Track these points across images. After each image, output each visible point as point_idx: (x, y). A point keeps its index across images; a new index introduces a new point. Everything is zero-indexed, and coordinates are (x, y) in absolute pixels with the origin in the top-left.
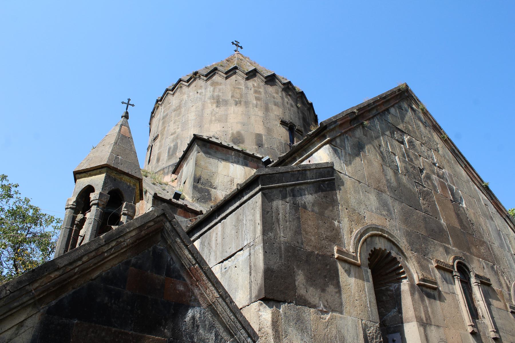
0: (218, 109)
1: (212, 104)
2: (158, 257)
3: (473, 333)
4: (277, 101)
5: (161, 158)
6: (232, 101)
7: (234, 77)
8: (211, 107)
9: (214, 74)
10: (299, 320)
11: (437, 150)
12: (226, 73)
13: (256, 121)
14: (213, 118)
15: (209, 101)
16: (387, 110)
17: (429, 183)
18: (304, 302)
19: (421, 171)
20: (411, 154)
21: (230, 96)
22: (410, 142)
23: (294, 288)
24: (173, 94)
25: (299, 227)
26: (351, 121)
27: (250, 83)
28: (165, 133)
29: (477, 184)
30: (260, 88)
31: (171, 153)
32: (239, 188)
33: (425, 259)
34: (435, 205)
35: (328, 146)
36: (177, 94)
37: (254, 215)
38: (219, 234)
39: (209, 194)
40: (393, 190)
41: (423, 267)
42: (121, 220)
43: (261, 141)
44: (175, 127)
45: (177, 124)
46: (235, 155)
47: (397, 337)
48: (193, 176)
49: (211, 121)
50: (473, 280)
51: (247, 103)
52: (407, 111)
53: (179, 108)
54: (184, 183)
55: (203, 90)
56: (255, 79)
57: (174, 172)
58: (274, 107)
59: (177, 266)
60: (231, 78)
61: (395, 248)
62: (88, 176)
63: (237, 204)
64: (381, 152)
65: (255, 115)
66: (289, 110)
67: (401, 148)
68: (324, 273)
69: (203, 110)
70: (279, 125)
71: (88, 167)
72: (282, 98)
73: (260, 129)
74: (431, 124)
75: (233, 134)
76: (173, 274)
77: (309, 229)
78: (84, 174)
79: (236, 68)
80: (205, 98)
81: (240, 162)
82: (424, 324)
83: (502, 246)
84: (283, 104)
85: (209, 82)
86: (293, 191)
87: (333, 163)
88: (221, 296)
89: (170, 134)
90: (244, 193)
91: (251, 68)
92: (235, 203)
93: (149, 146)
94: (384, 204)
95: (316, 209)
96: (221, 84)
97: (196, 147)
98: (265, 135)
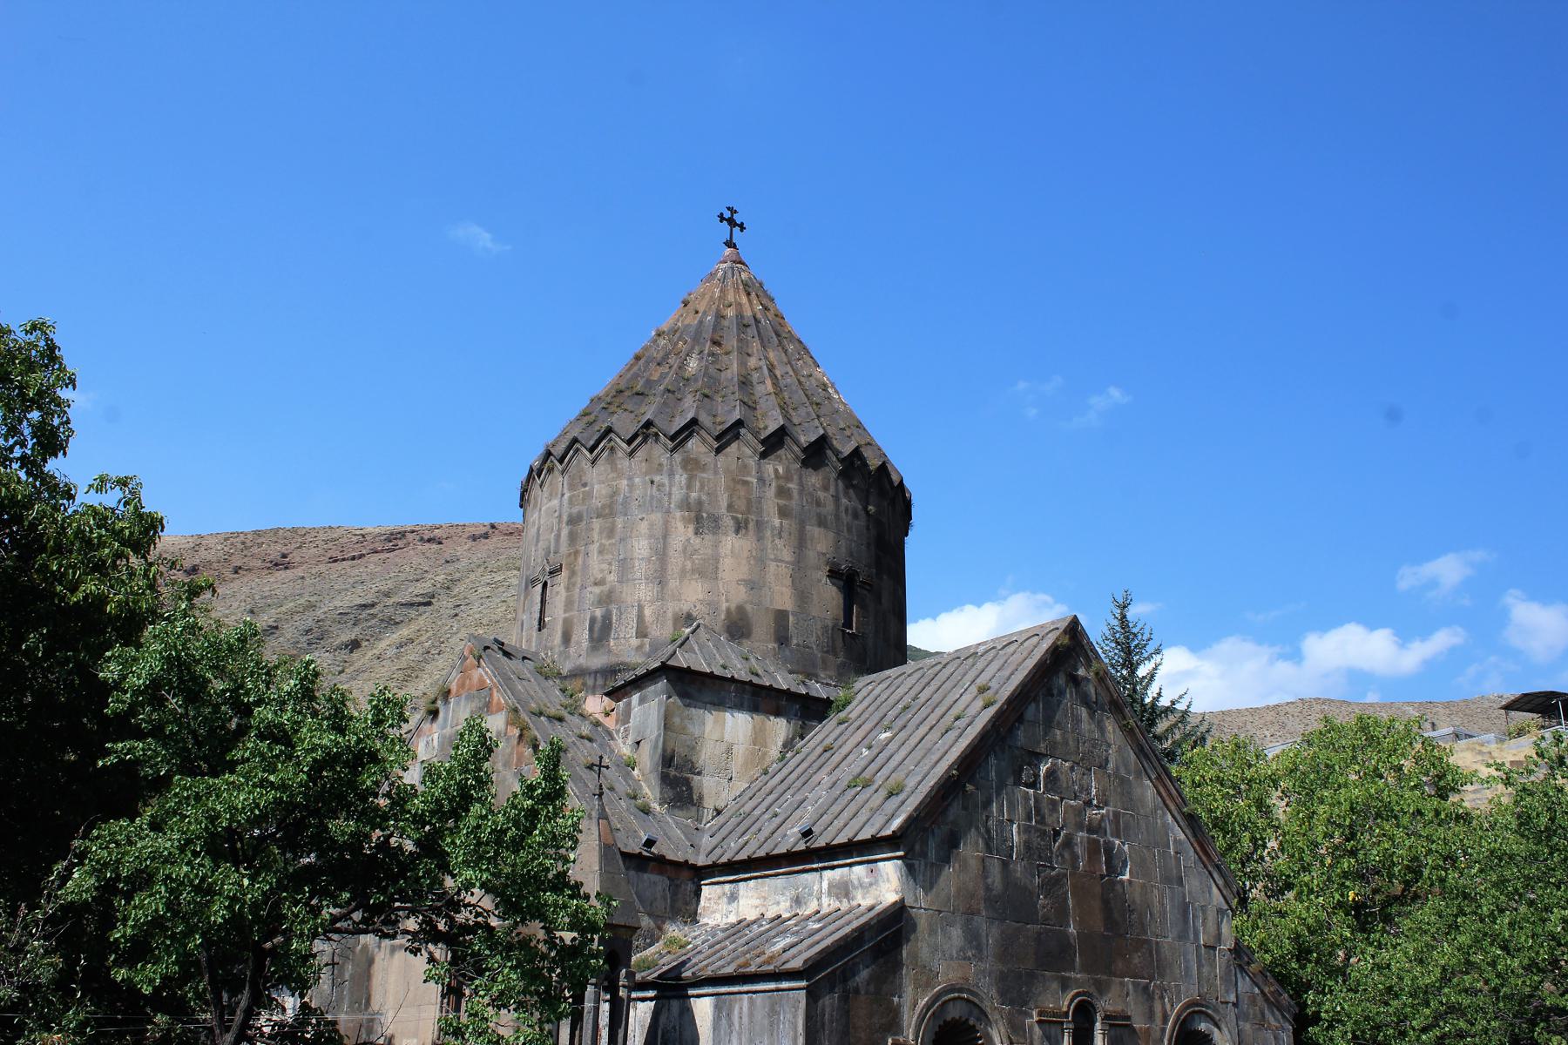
0: (698, 540)
1: (686, 521)
4: (824, 511)
5: (574, 638)
6: (728, 522)
7: (734, 445)
8: (682, 533)
11: (1103, 766)
12: (718, 438)
14: (689, 565)
15: (678, 514)
16: (1021, 719)
17: (1067, 855)
19: (1057, 834)
20: (1044, 804)
21: (724, 503)
22: (1051, 774)
24: (593, 462)
26: (944, 798)
27: (771, 467)
29: (1173, 807)
30: (788, 478)
33: (1021, 1012)
34: (1066, 899)
36: (602, 465)
37: (795, 1017)
38: (745, 1009)
39: (690, 789)
40: (991, 900)
48: (660, 751)
50: (1098, 1025)
51: (760, 525)
52: (1062, 693)
53: (608, 512)
55: (666, 481)
56: (781, 452)
57: (607, 694)
58: (814, 531)
60: (728, 450)
61: (976, 1011)
63: (772, 986)
64: (988, 831)
65: (776, 560)
66: (850, 530)
67: (1026, 797)
69: (665, 537)
70: (825, 579)
72: (836, 498)
73: (783, 598)
74: (1107, 699)
75: (728, 610)
79: (739, 423)
83: (1182, 936)
84: (837, 517)
85: (678, 457)
87: (902, 900)
94: (973, 938)
95: (872, 988)
96: (703, 468)
97: (662, 684)
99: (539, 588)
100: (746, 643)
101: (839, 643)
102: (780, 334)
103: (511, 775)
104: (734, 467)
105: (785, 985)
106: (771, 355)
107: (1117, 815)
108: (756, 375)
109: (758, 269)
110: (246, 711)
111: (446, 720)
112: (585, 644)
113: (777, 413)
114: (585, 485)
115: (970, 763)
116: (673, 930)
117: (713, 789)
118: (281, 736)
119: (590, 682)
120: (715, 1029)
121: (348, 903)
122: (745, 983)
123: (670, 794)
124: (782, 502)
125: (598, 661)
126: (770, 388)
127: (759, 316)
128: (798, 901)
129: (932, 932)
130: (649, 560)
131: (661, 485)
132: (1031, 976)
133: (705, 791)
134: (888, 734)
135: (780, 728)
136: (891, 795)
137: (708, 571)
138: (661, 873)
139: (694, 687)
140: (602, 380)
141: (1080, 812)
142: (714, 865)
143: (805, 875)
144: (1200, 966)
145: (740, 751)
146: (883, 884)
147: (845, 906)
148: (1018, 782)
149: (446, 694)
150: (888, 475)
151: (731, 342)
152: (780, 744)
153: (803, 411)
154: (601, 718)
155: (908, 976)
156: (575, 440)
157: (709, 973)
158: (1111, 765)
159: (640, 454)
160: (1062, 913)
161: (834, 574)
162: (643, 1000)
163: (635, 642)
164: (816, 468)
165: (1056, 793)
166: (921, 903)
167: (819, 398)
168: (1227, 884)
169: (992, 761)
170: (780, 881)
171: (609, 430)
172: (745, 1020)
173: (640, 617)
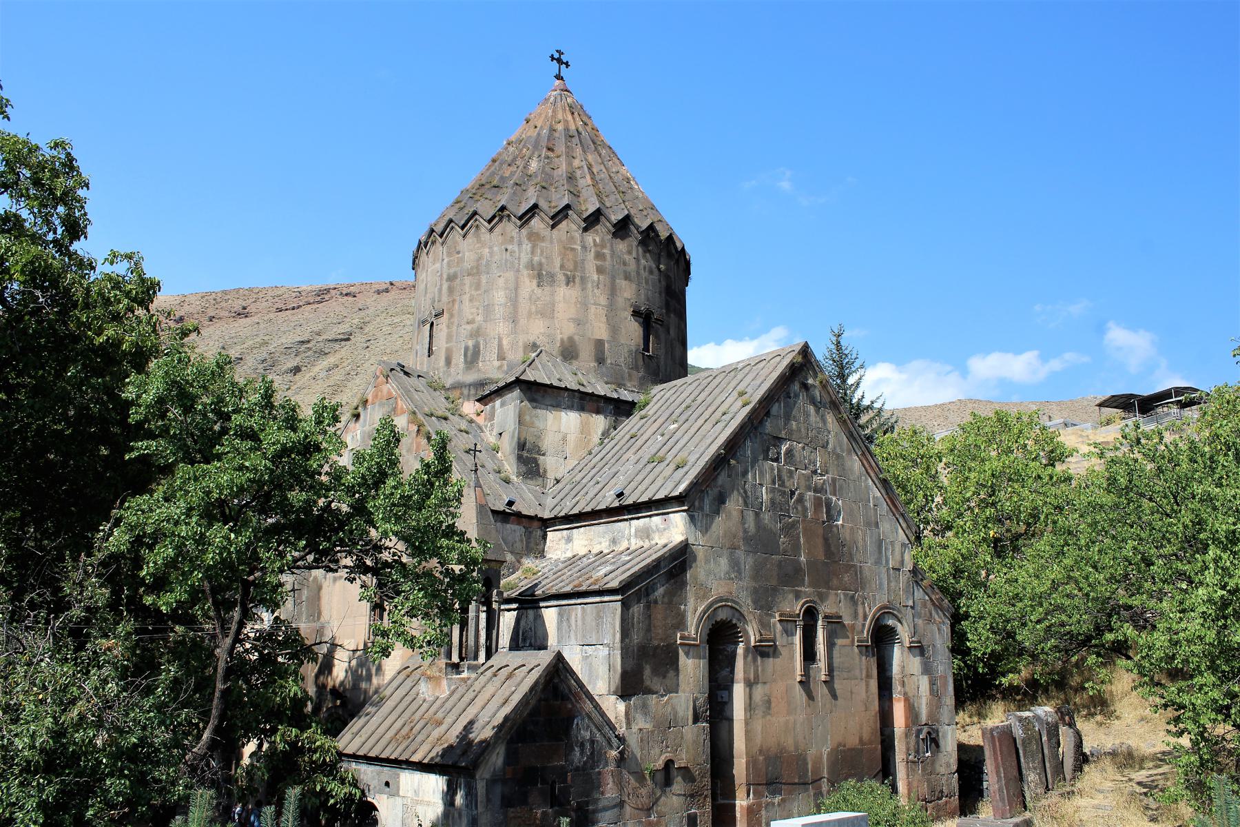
2: (556, 688)
3: (800, 682)
5: (454, 362)
6: (561, 278)
7: (564, 223)
8: (528, 285)
9: (533, 216)
10: (644, 707)
11: (825, 446)
12: (552, 218)
14: (533, 310)
15: (525, 272)
16: (768, 414)
18: (649, 691)
19: (793, 493)
21: (557, 263)
22: (789, 452)
23: (642, 681)
25: (649, 625)
26: (715, 469)
27: (590, 238)
30: (603, 246)
33: (767, 615)
39: (537, 465)
40: (747, 539)
41: (764, 625)
45: (477, 304)
47: (725, 694)
50: (820, 623)
51: (583, 280)
52: (797, 396)
53: (475, 271)
55: (516, 249)
57: (478, 400)
58: (622, 283)
61: (737, 614)
63: (598, 599)
64: (745, 492)
66: (647, 282)
67: (772, 469)
68: (666, 660)
69: (516, 289)
72: (637, 260)
73: (600, 331)
74: (828, 400)
75: (562, 340)
76: (565, 698)
79: (568, 207)
82: (750, 684)
83: (878, 562)
84: (638, 273)
85: (524, 231)
86: (647, 589)
94: (735, 565)
95: (666, 600)
96: (543, 239)
97: (517, 393)
100: (575, 363)
101: (641, 362)
102: (596, 143)
103: (413, 458)
105: (606, 598)
106: (590, 158)
107: (834, 480)
108: (578, 173)
109: (578, 96)
110: (227, 417)
112: (462, 365)
113: (594, 199)
114: (458, 253)
115: (733, 445)
116: (528, 563)
117: (552, 464)
118: (250, 435)
120: (559, 629)
121: (304, 548)
123: (524, 469)
124: (599, 263)
125: (471, 378)
126: (589, 182)
127: (580, 129)
128: (614, 541)
129: (707, 561)
130: (505, 305)
132: (775, 590)
133: (548, 467)
134: (676, 426)
135: (599, 422)
136: (678, 467)
137: (547, 312)
138: (519, 524)
139: (537, 393)
140: (469, 179)
141: (809, 478)
142: (556, 518)
144: (889, 582)
145: (572, 439)
146: (673, 529)
147: (647, 544)
148: (766, 458)
150: (674, 243)
151: (561, 148)
153: (612, 198)
154: (474, 417)
155: (691, 593)
156: (451, 221)
157: (553, 591)
158: (830, 446)
159: (498, 230)
160: (796, 548)
161: (636, 313)
162: (509, 610)
163: (496, 363)
164: (623, 239)
165: (793, 465)
166: (700, 543)
167: (624, 188)
168: (909, 527)
169: (748, 443)
171: (475, 213)
172: (580, 622)
173: (500, 346)
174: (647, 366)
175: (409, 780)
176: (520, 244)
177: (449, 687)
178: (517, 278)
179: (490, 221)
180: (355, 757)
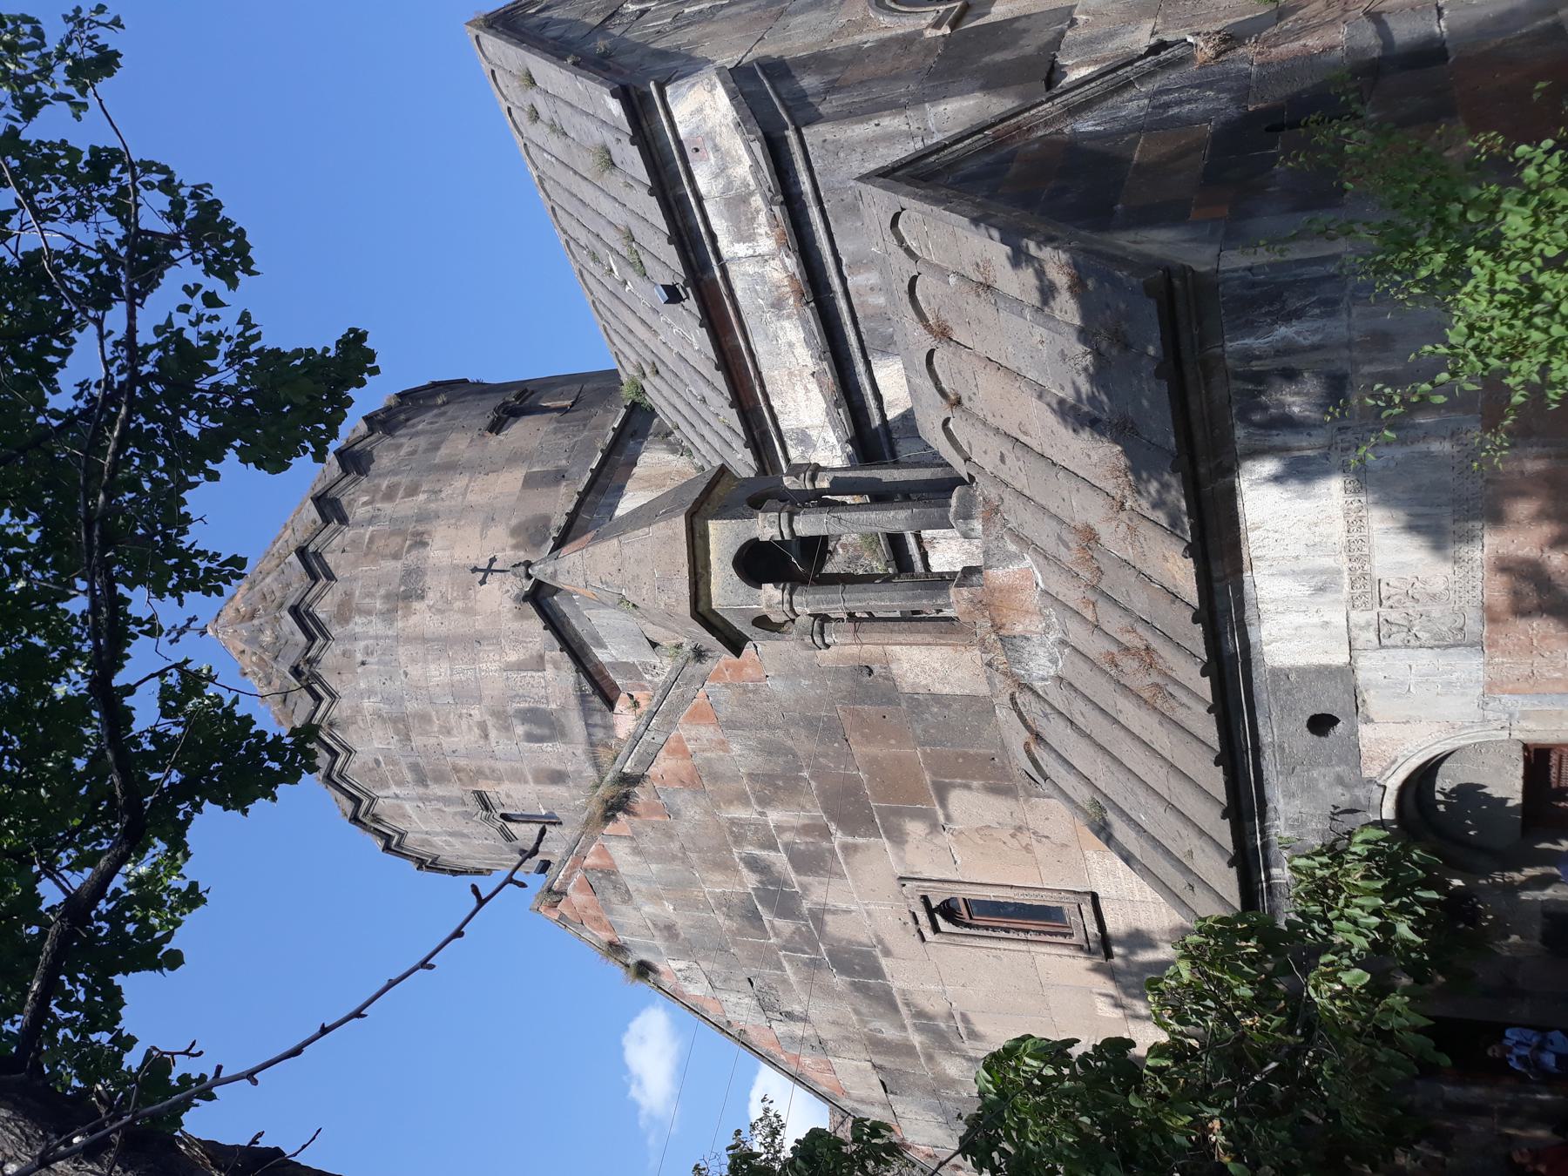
0: (431, 594)
1: (409, 613)
5: (555, 765)
6: (411, 559)
7: (330, 559)
8: (422, 618)
12: (315, 578)
13: (482, 491)
14: (458, 604)
15: (400, 624)
21: (389, 565)
24: (349, 751)
28: (473, 765)
30: (377, 488)
31: (546, 732)
32: (780, 198)
35: (669, 90)
36: (351, 738)
42: (826, 485)
43: (545, 474)
44: (465, 727)
45: (453, 719)
46: (591, 513)
49: (468, 611)
51: (423, 517)
54: (654, 645)
55: (361, 644)
56: (344, 501)
57: (610, 704)
59: (988, 159)
60: (331, 565)
62: (709, 574)
65: (464, 494)
66: (454, 418)
69: (424, 640)
70: (501, 437)
71: (686, 569)
73: (510, 481)
75: (516, 547)
77: (888, 68)
78: (701, 586)
79: (301, 552)
80: (387, 637)
81: (610, 501)
85: (335, 630)
87: (720, 71)
88: (1048, 100)
89: (482, 742)
90: (794, 190)
91: (312, 512)
92: (810, 224)
93: (502, 830)
95: (834, 70)
96: (348, 595)
98: (531, 465)
99: (511, 826)
104: (351, 556)
105: (806, 186)
111: (649, 949)
112: (559, 747)
114: (377, 762)
119: (599, 734)
122: (828, 287)
130: (451, 660)
131: (368, 652)
143: (739, 294)
146: (702, 110)
149: (616, 949)
152: (671, 457)
159: (333, 682)
161: (496, 427)
163: (550, 672)
170: (760, 348)
174: (591, 404)
175: (1289, 629)
176: (355, 638)
177: (1011, 558)
178: (410, 640)
179: (318, 699)
180: (1248, 860)
